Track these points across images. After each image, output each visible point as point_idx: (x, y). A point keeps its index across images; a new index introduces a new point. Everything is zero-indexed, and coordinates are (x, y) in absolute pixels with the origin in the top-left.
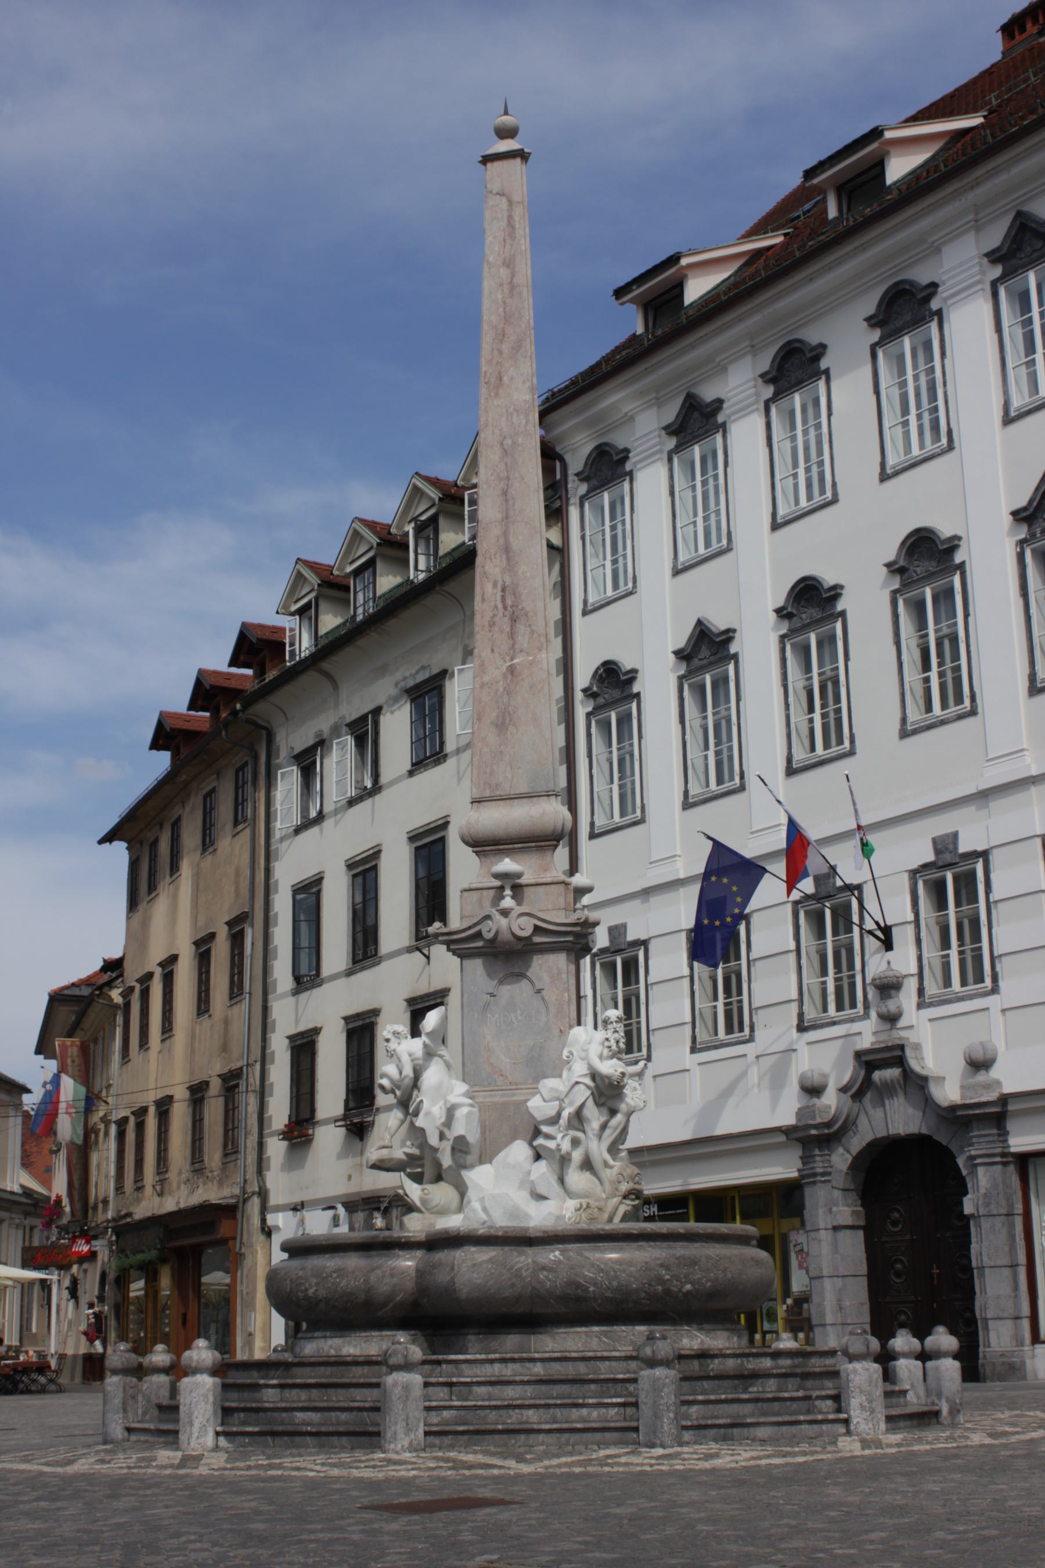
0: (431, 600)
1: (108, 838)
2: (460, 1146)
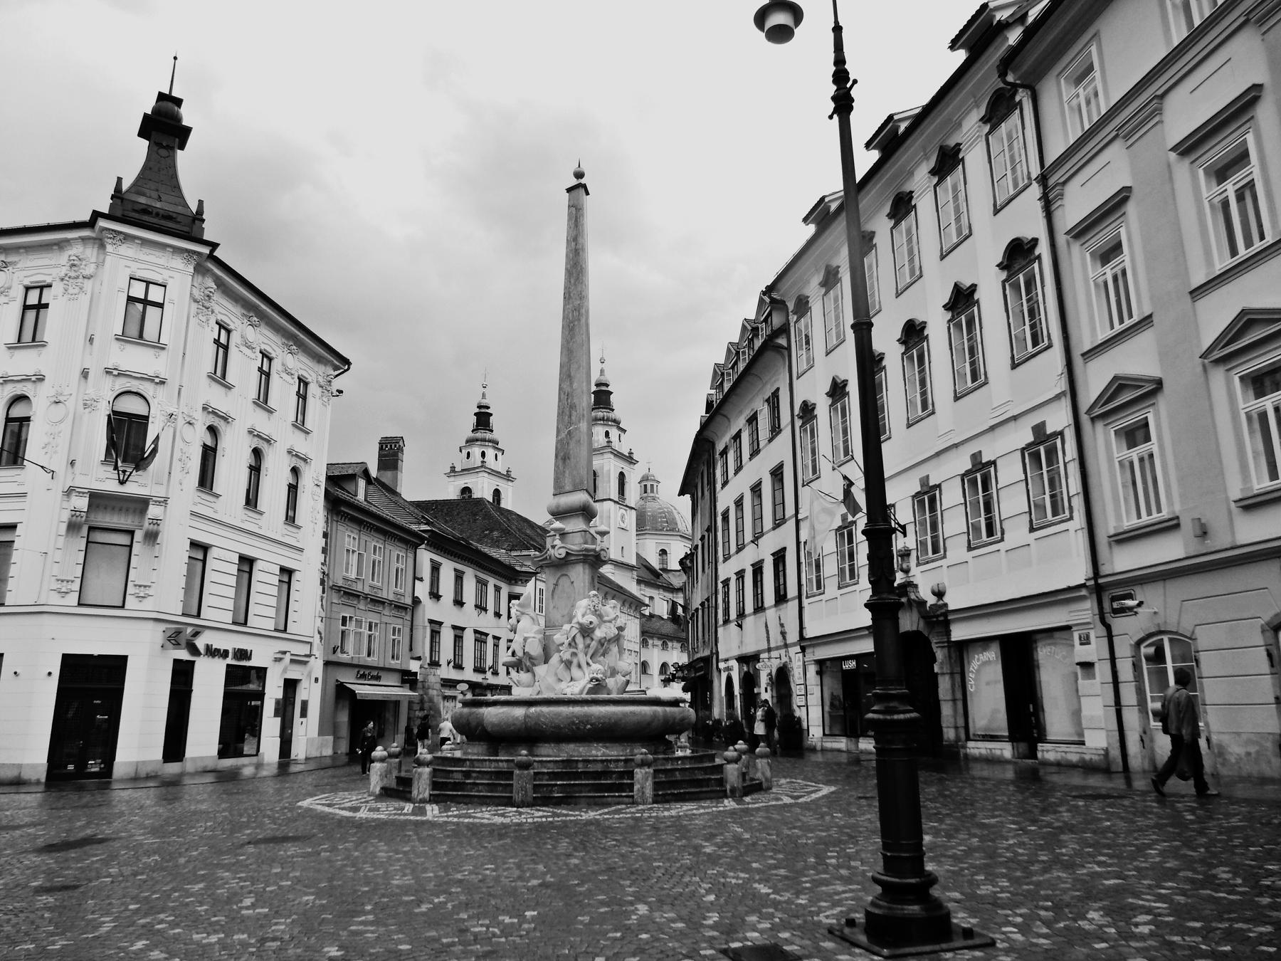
0: (750, 378)
1: (682, 493)
2: (531, 658)
